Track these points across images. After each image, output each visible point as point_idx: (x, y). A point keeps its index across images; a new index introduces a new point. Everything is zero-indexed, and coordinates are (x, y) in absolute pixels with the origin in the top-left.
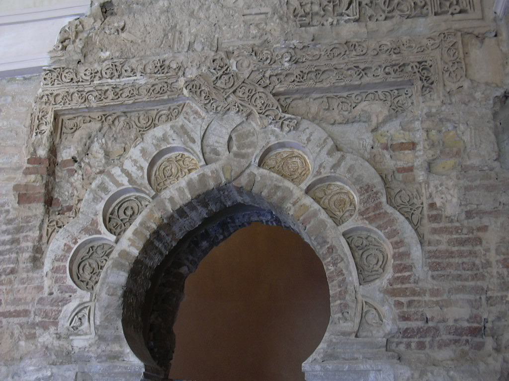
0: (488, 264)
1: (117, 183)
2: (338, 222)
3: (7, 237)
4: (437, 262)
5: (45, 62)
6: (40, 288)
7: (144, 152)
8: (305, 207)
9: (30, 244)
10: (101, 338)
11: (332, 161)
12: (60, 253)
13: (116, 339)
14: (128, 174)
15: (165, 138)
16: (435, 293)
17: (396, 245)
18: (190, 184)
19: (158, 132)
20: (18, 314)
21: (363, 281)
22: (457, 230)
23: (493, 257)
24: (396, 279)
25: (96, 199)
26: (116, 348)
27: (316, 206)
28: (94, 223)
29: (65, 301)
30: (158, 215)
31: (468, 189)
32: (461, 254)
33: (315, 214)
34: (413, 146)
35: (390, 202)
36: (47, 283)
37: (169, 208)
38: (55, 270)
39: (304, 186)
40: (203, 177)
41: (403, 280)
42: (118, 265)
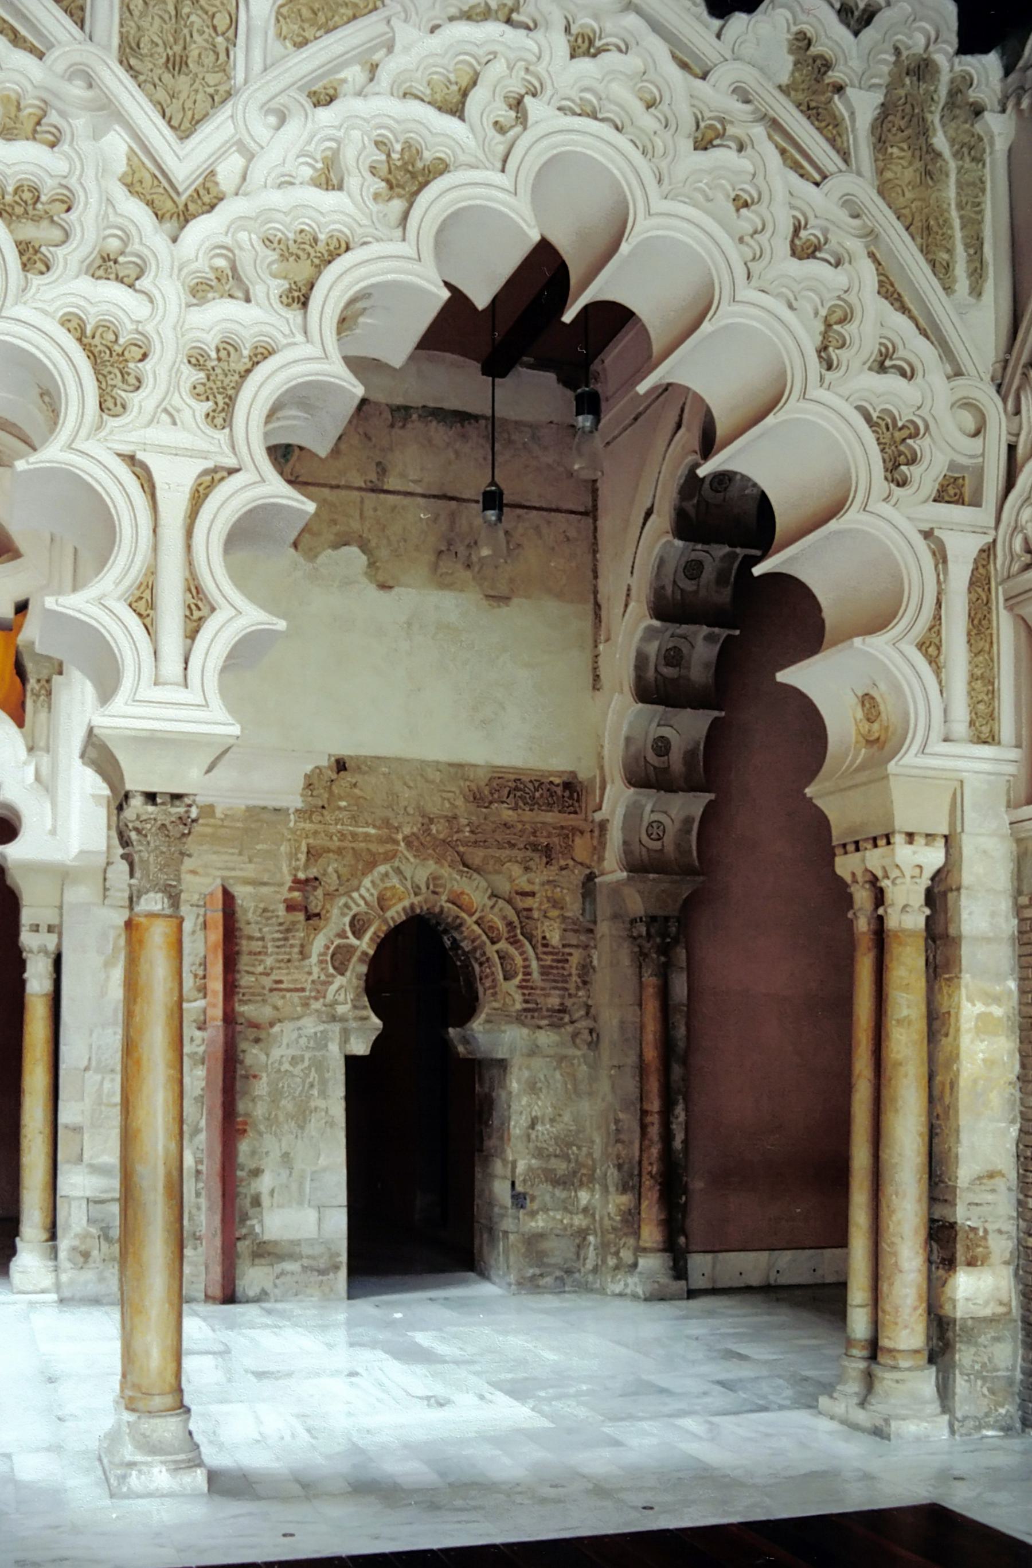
0: (570, 975)
1: (358, 905)
2: (493, 943)
3: (280, 936)
4: (545, 971)
5: (298, 803)
6: (310, 973)
7: (372, 882)
8: (473, 931)
9: (297, 942)
10: (355, 1007)
11: (490, 903)
12: (322, 950)
13: (365, 1008)
14: (363, 898)
15: (387, 875)
16: (543, 989)
17: (525, 960)
18: (404, 909)
19: (382, 869)
20: (297, 990)
21: (506, 979)
22: (557, 954)
23: (574, 972)
24: (524, 980)
25: (343, 915)
26: (364, 1013)
27: (480, 931)
28: (344, 931)
29: (331, 983)
30: (385, 928)
31: (565, 930)
32: (557, 968)
33: (479, 936)
34: (533, 894)
35: (522, 934)
36: (316, 970)
37: (392, 924)
38: (321, 962)
39: (474, 918)
40: (412, 906)
41: (527, 981)
42: (361, 960)
